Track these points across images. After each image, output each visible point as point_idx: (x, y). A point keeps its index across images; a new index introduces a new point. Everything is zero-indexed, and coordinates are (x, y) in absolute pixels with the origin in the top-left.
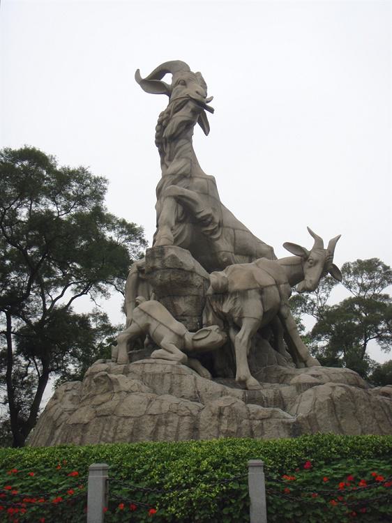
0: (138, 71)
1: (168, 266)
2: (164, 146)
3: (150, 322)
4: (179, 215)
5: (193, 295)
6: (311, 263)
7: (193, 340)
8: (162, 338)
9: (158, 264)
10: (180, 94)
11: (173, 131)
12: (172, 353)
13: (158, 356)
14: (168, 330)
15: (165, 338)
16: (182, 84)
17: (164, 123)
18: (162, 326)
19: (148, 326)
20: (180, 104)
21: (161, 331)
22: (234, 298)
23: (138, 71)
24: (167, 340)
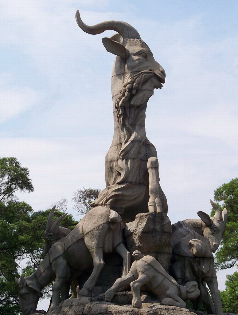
0: (78, 13)
1: (166, 230)
2: (127, 110)
3: (156, 275)
4: (141, 178)
5: (170, 253)
6: (215, 231)
7: (187, 292)
8: (168, 289)
9: (158, 227)
10: (141, 66)
11: (143, 103)
12: (177, 301)
13: (170, 304)
14: (172, 284)
15: (170, 289)
16: (143, 56)
17: (134, 92)
18: (167, 279)
19: (154, 277)
20: (148, 77)
21: (166, 283)
22: (210, 262)
23: (78, 13)
24: (172, 290)
